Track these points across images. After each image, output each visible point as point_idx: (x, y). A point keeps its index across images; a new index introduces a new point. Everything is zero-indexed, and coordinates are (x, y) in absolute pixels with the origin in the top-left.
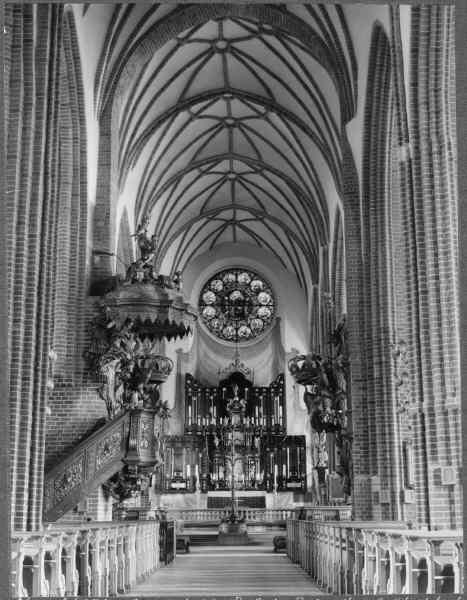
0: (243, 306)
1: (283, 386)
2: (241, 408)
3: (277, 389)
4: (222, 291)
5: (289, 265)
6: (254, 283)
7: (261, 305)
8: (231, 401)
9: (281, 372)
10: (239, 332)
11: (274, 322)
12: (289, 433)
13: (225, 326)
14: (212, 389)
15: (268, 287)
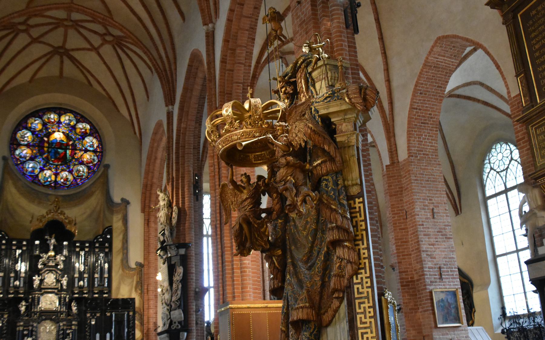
0: (66, 149)
1: (110, 241)
2: (57, 265)
3: (102, 244)
4: (41, 131)
5: (124, 111)
6: (80, 126)
7: (86, 151)
8: (45, 256)
9: (107, 225)
10: (58, 179)
11: (102, 169)
12: (114, 296)
13: (42, 170)
14: (20, 242)
15: (94, 132)
